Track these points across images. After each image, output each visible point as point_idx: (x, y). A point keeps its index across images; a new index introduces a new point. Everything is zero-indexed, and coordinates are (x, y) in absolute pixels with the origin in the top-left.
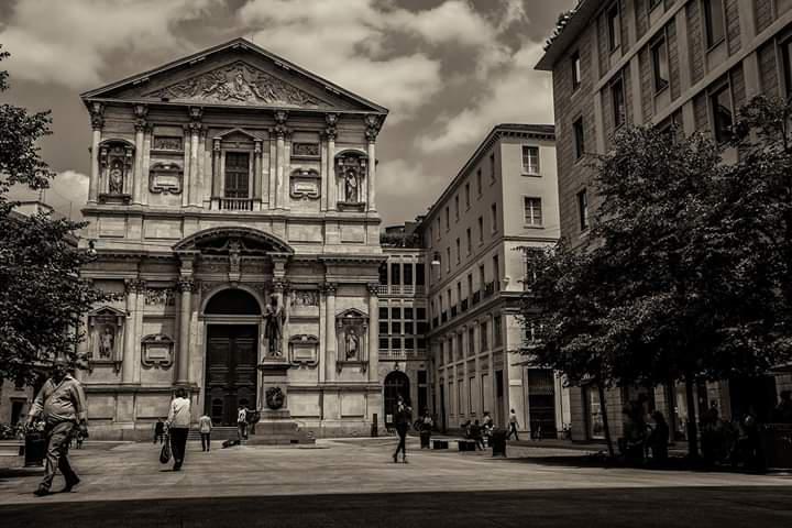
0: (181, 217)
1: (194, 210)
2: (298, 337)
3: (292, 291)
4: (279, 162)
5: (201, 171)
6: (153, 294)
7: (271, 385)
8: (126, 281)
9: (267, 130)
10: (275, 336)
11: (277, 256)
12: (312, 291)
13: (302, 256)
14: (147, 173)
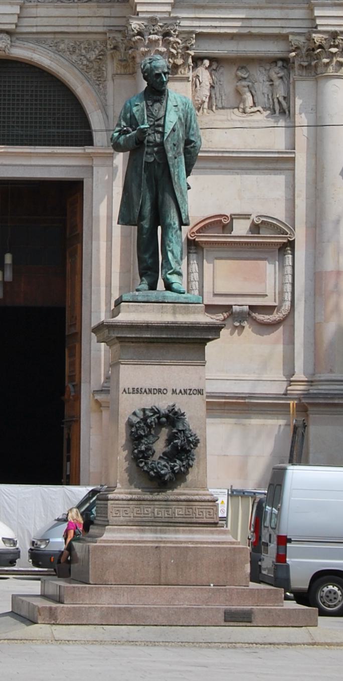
2: (222, 224)
3: (198, 60)
7: (149, 401)
10: (158, 217)
12: (274, 61)
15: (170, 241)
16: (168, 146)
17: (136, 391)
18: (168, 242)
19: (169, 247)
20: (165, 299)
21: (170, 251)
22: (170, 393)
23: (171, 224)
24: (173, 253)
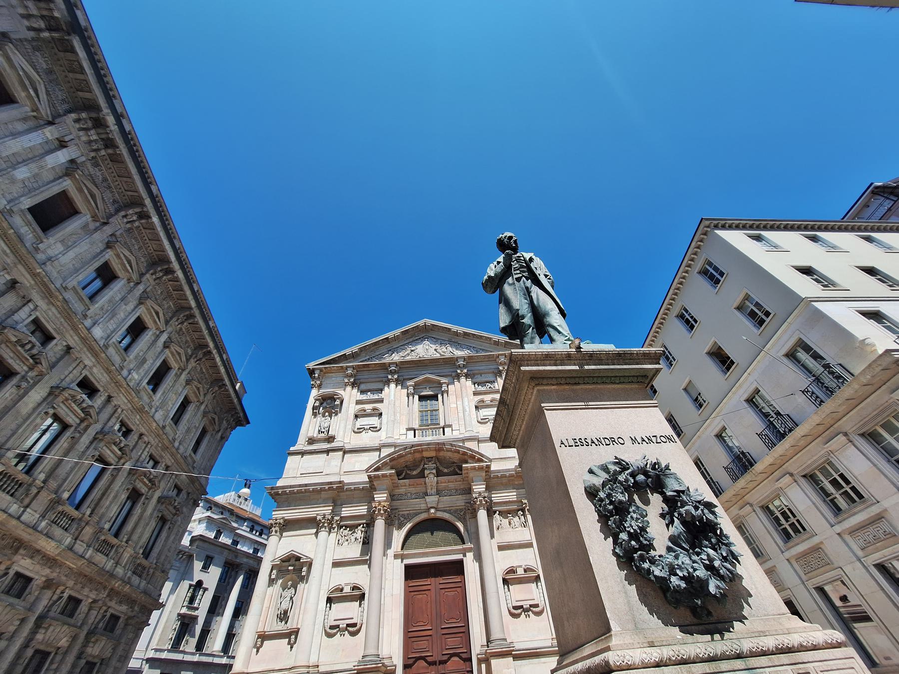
0: (379, 449)
1: (390, 441)
2: (512, 571)
4: (464, 395)
5: (398, 410)
6: (346, 532)
8: (319, 518)
9: (451, 375)
11: (474, 468)
13: (499, 471)
14: (352, 417)
17: (580, 443)
22: (628, 442)
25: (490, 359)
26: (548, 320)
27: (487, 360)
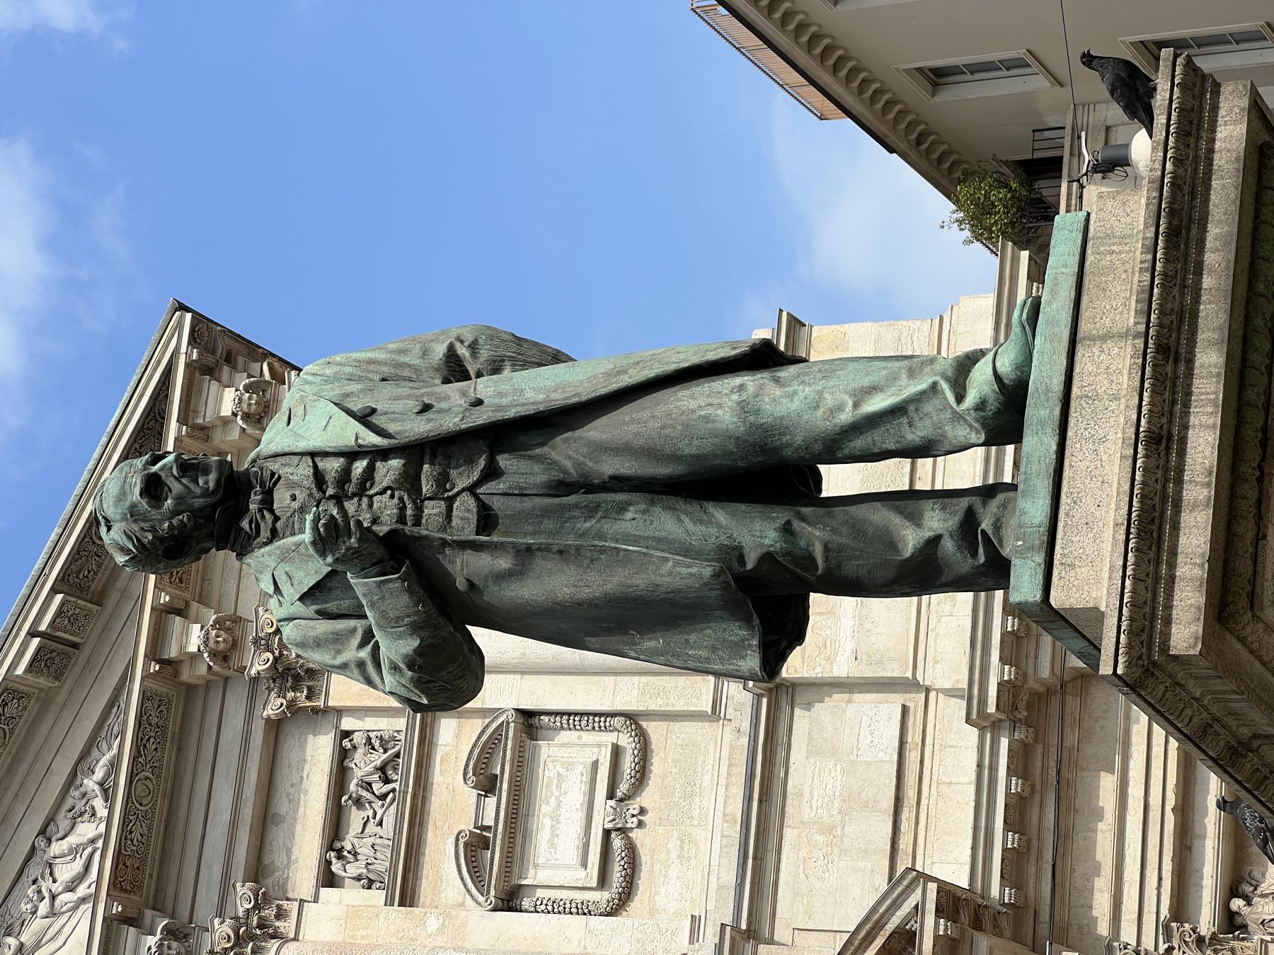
15: (817, 407)
16: (418, 428)
18: (820, 413)
19: (840, 408)
20: (1048, 391)
21: (856, 405)
23: (742, 405)
24: (873, 390)
25: (173, 726)
26: (799, 440)
27: (168, 754)
